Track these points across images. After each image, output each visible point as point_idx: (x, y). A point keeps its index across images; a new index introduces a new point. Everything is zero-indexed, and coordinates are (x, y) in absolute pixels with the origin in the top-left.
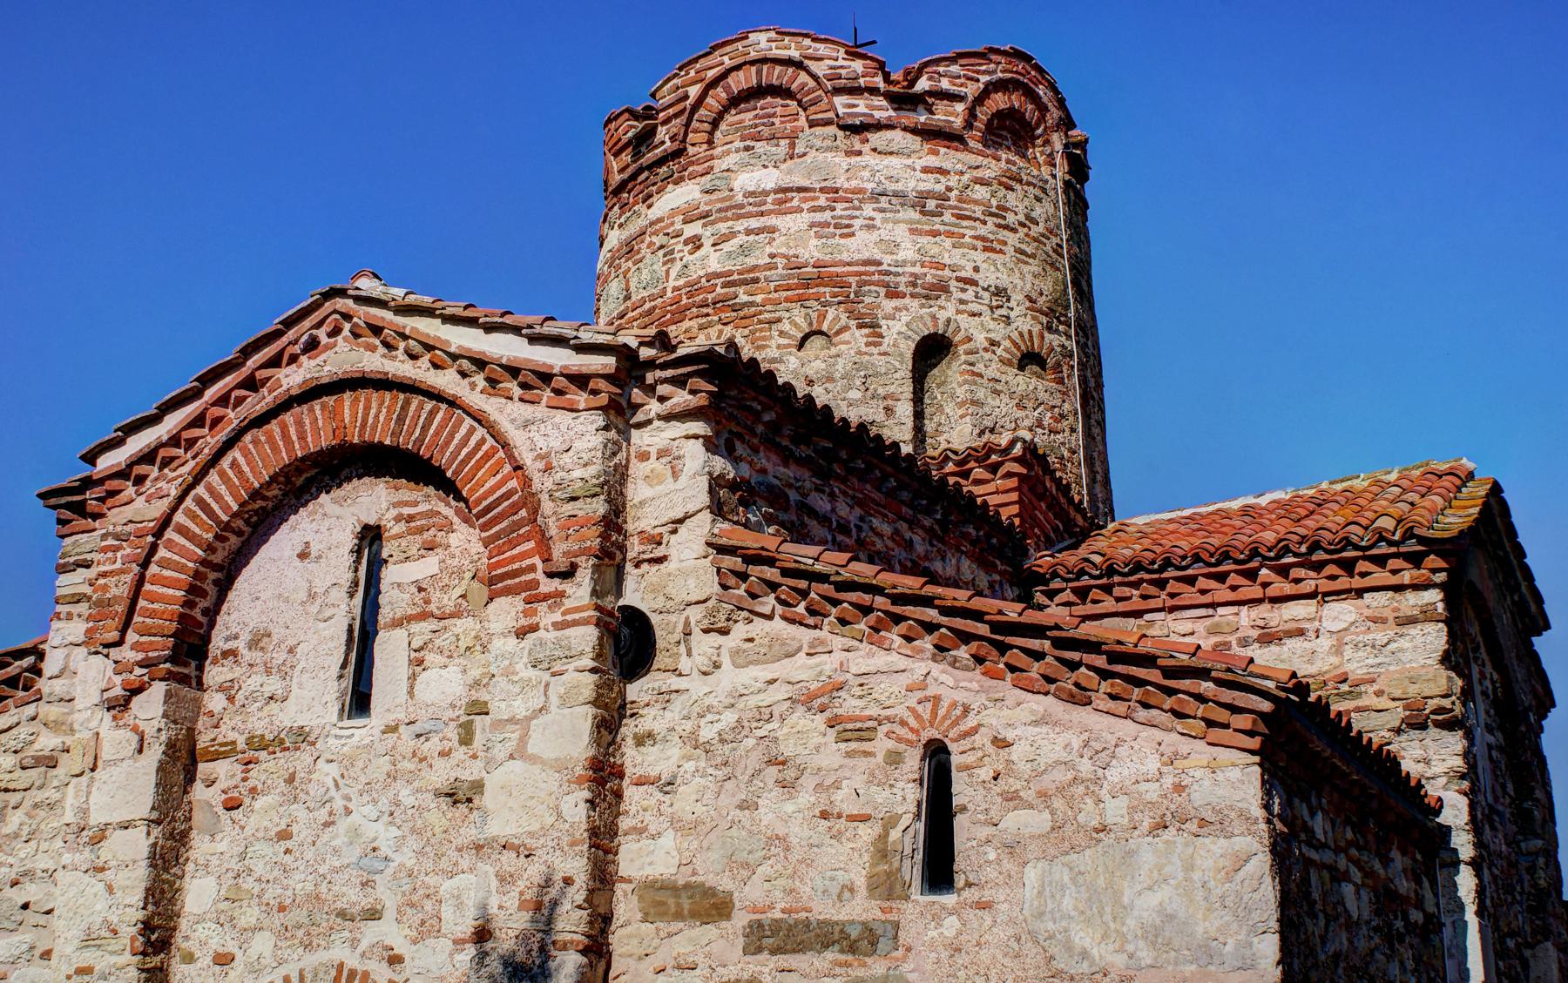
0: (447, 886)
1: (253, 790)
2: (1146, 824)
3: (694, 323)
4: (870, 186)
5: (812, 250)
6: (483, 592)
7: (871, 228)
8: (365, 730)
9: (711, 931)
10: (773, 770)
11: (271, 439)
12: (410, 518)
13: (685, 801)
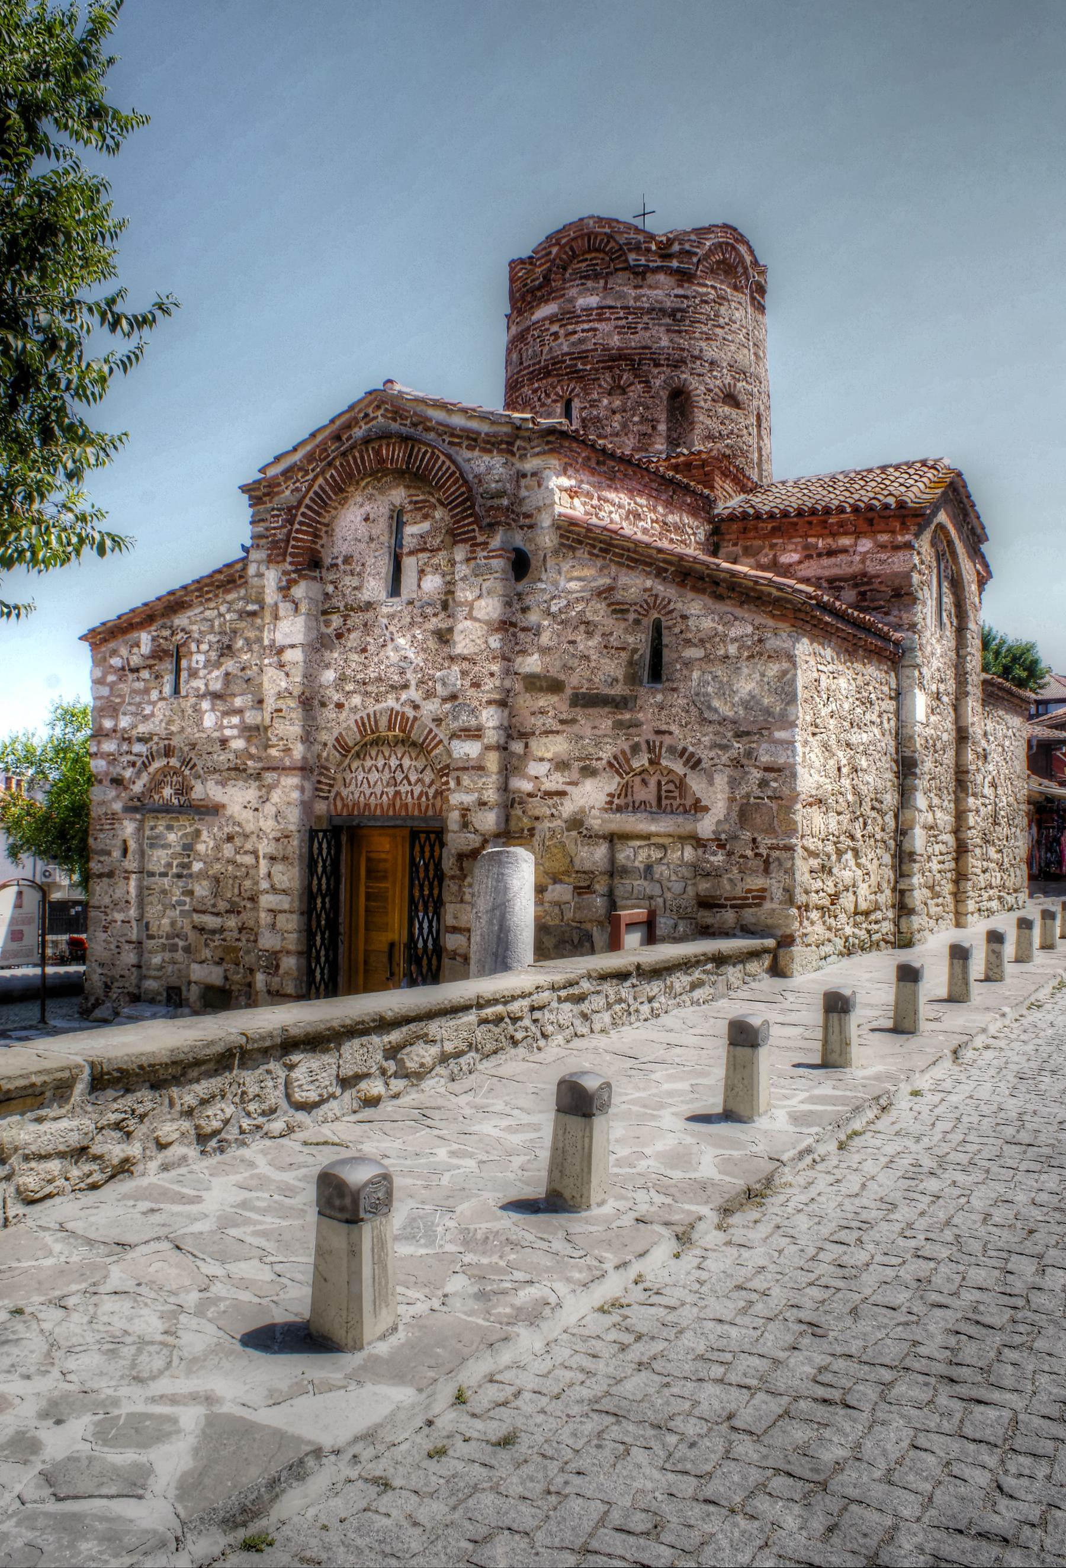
0: (438, 674)
1: (349, 630)
2: (746, 654)
3: (555, 380)
4: (646, 305)
5: (615, 341)
6: (449, 540)
7: (646, 329)
8: (396, 605)
9: (554, 699)
10: (582, 628)
11: (348, 462)
12: (416, 502)
13: (545, 639)
